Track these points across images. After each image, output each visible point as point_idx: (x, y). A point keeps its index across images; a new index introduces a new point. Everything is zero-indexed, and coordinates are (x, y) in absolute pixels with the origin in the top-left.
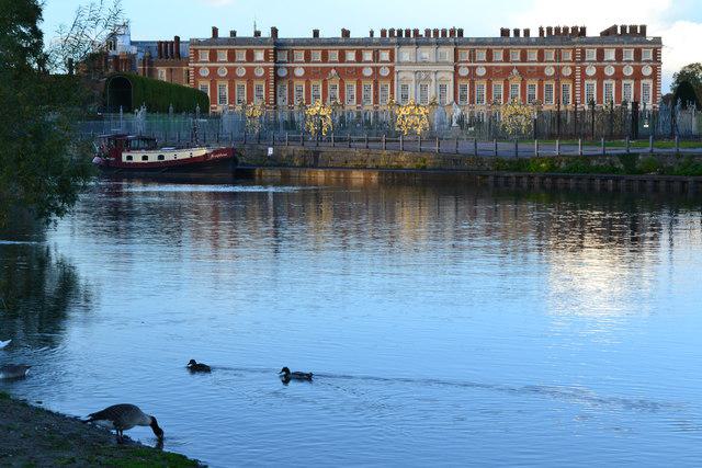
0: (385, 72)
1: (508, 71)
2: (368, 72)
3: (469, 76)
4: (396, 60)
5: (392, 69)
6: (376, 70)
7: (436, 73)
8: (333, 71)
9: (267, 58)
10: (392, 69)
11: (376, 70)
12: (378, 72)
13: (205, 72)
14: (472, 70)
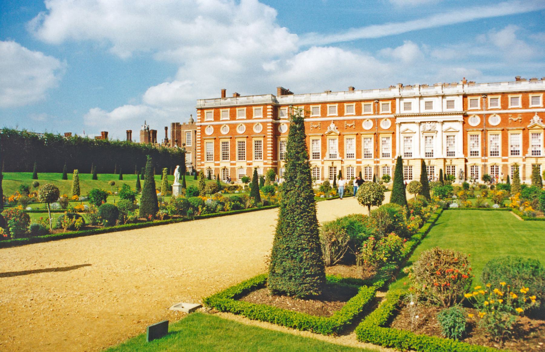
0: (385, 125)
1: (528, 117)
2: (368, 126)
3: (480, 125)
4: (397, 112)
5: (393, 120)
6: (376, 122)
7: (443, 122)
8: (332, 126)
9: (265, 115)
10: (393, 120)
11: (376, 122)
12: (378, 124)
13: (209, 132)
14: (484, 117)
